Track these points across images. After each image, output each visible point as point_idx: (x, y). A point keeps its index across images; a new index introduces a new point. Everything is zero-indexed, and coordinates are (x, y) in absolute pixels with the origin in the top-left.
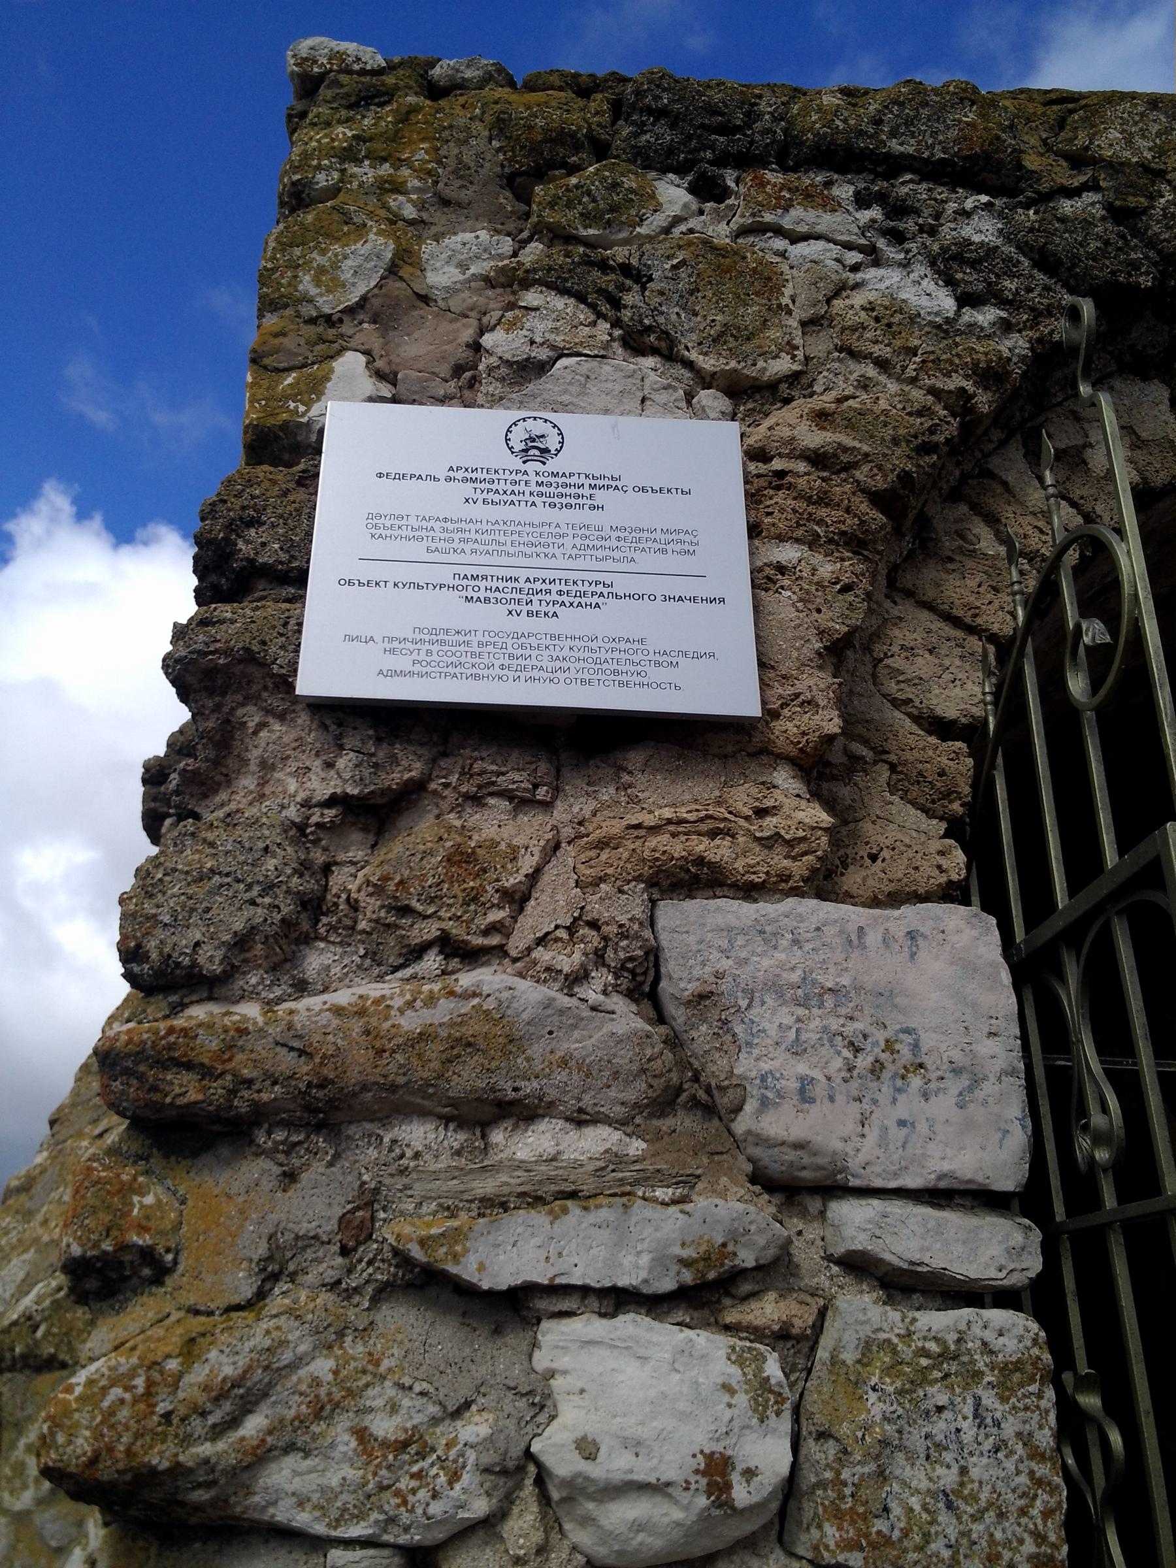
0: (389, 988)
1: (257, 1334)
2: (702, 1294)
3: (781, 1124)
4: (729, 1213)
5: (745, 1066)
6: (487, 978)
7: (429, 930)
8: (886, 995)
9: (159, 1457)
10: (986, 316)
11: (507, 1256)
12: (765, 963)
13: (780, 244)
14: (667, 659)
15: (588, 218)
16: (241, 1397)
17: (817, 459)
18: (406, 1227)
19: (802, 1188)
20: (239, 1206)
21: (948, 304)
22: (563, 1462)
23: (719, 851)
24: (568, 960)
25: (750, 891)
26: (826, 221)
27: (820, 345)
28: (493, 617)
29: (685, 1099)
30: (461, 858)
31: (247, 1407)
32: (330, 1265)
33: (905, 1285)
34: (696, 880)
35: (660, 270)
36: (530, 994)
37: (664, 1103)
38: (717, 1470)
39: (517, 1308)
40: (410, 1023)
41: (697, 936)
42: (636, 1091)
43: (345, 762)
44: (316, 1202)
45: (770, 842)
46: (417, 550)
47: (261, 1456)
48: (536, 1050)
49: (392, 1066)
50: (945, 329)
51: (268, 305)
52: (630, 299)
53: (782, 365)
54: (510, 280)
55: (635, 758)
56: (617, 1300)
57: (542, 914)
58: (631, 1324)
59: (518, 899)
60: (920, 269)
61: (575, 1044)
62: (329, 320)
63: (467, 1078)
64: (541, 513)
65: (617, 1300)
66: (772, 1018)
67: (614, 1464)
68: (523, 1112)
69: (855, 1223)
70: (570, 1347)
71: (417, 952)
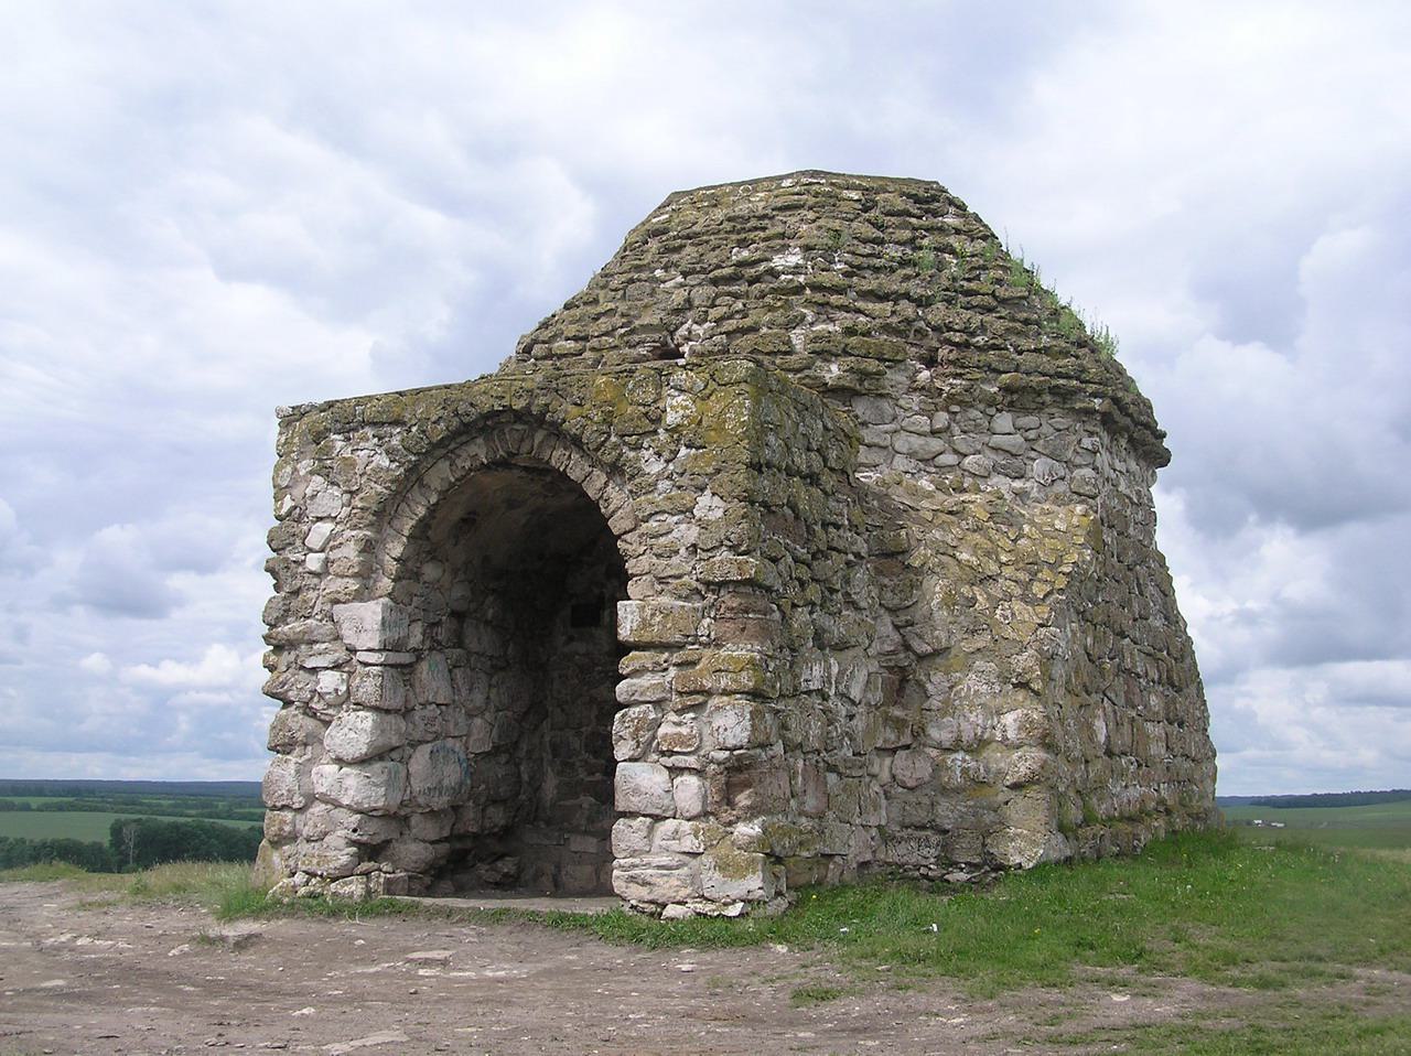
1: (285, 675)
2: (337, 667)
4: (342, 655)
6: (308, 621)
9: (274, 691)
10: (393, 466)
11: (309, 664)
13: (359, 452)
17: (361, 509)
19: (352, 650)
20: (287, 657)
21: (388, 463)
24: (319, 617)
25: (344, 603)
26: (367, 445)
27: (364, 479)
30: (305, 601)
31: (285, 684)
33: (366, 665)
34: (337, 602)
35: (335, 465)
36: (315, 622)
37: (335, 639)
38: (336, 690)
39: (314, 670)
42: (332, 637)
44: (292, 657)
45: (346, 594)
47: (287, 691)
48: (315, 633)
50: (388, 469)
51: (275, 487)
53: (356, 488)
54: (311, 473)
56: (327, 668)
57: (316, 610)
59: (313, 608)
60: (384, 454)
61: (321, 631)
63: (306, 637)
65: (327, 668)
67: (324, 690)
68: (316, 642)
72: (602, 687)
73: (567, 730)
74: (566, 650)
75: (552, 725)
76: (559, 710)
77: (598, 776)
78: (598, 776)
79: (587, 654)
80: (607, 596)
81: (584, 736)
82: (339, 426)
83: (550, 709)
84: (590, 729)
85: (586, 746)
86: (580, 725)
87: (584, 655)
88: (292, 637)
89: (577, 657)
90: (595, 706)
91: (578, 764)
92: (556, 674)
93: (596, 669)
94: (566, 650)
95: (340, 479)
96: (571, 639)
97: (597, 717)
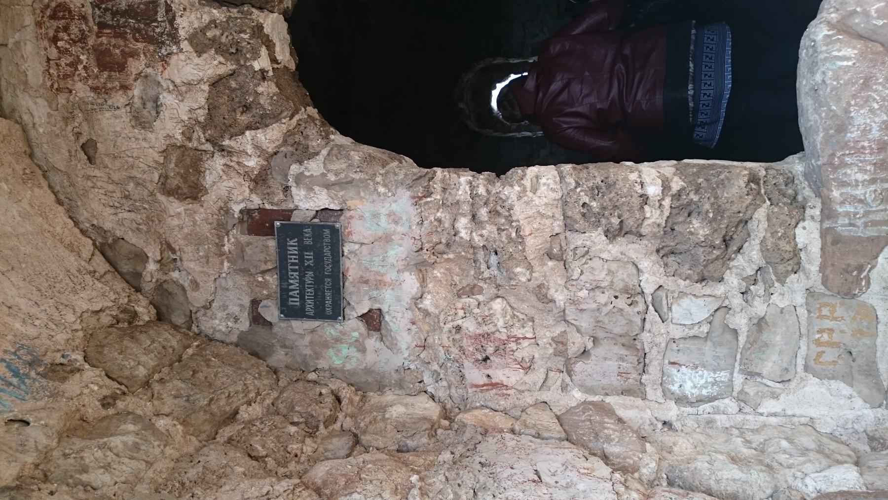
72: (520, 212)
73: (645, 336)
74: (405, 340)
75: (625, 392)
76: (579, 367)
77: (808, 235)
78: (808, 235)
79: (421, 268)
80: (256, 201)
81: (670, 283)
83: (578, 395)
84: (645, 264)
85: (702, 279)
86: (633, 293)
87: (423, 281)
89: (427, 303)
90: (578, 240)
91: (759, 308)
92: (475, 375)
93: (464, 234)
94: (405, 340)
96: (373, 320)
97: (611, 235)
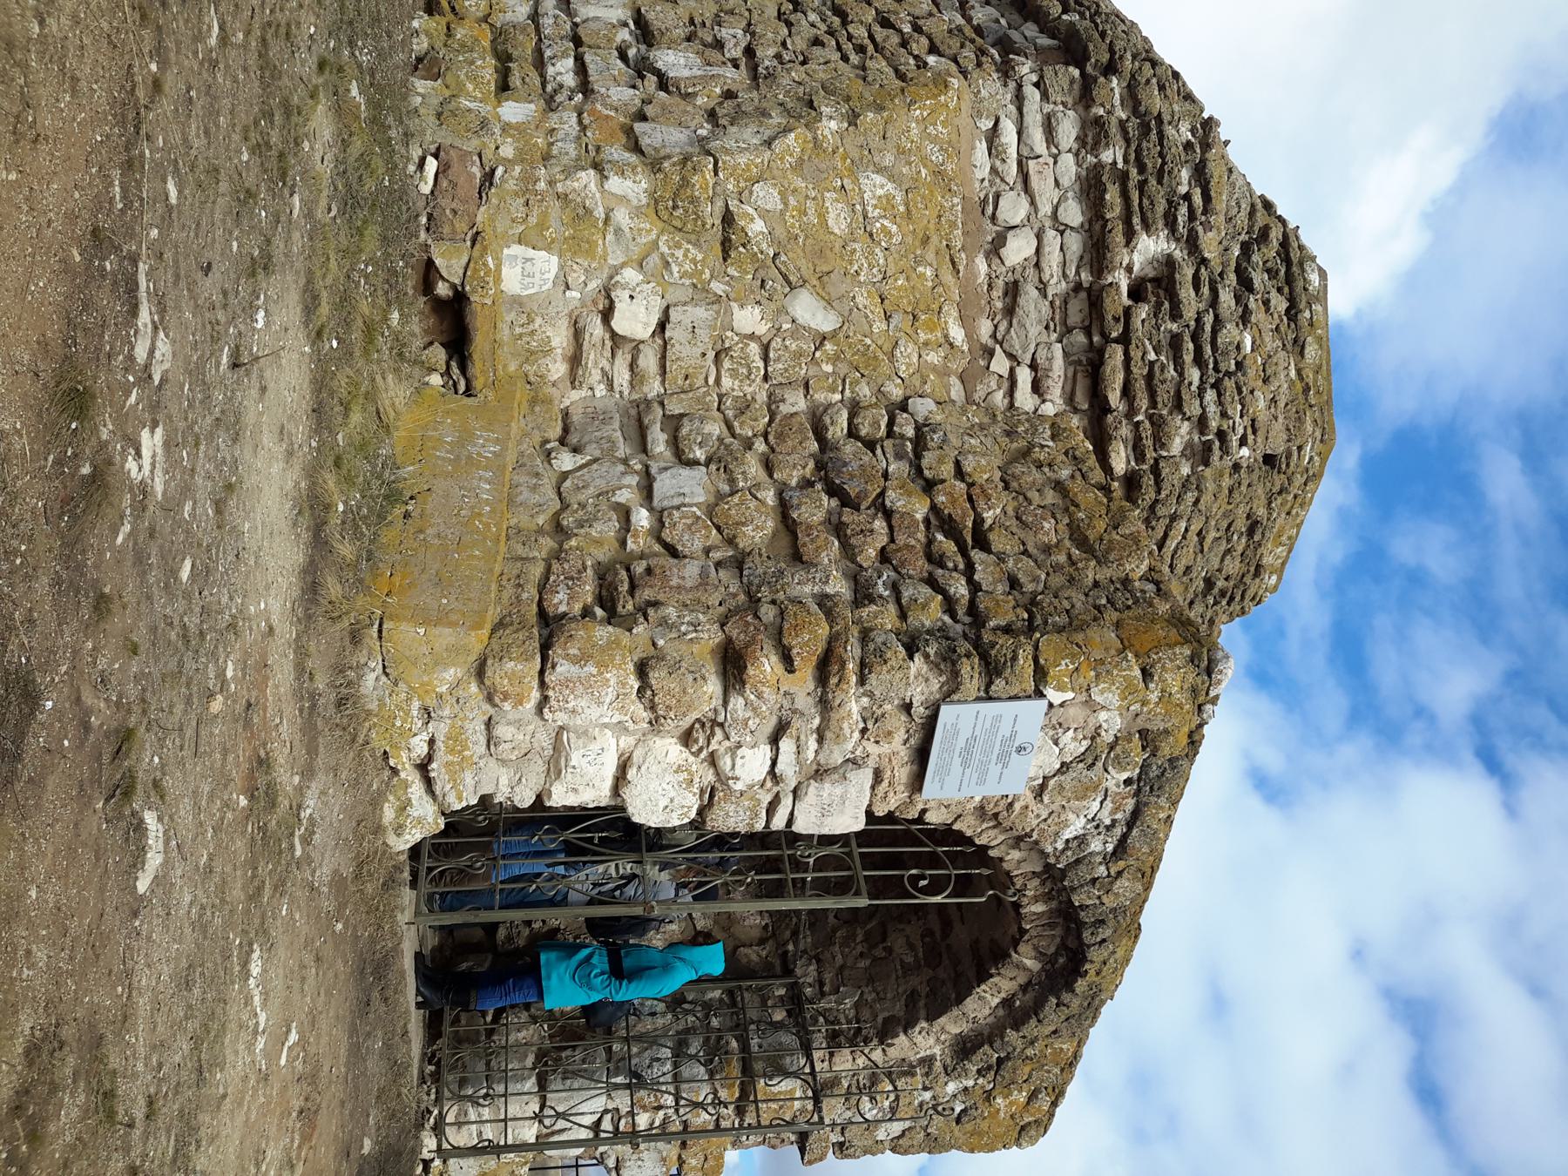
0: (856, 716)
3: (812, 790)
5: (827, 785)
6: (857, 735)
7: (870, 726)
8: (842, 812)
11: (786, 745)
12: (853, 791)
14: (942, 781)
15: (1117, 756)
16: (760, 696)
18: (796, 723)
22: (740, 752)
23: (885, 784)
25: (873, 788)
28: (961, 743)
29: (820, 773)
32: (786, 705)
34: (878, 776)
35: (1091, 774)
40: (845, 725)
41: (865, 777)
43: (922, 709)
46: (988, 725)
49: (833, 723)
52: (1081, 765)
55: (915, 767)
58: (769, 763)
62: (1088, 690)
64: (996, 751)
66: (838, 790)
67: (739, 762)
68: (821, 740)
69: (787, 801)
70: (765, 751)
71: (865, 721)
82: (1154, 772)
88: (834, 715)
95: (1066, 779)
